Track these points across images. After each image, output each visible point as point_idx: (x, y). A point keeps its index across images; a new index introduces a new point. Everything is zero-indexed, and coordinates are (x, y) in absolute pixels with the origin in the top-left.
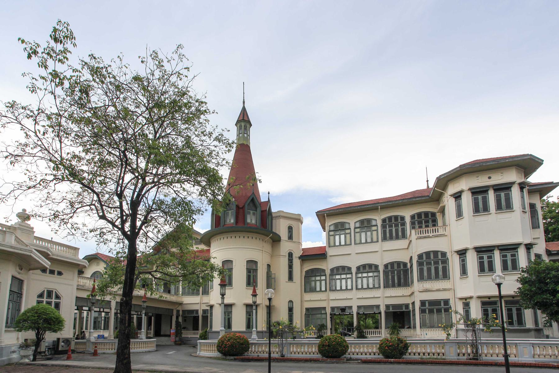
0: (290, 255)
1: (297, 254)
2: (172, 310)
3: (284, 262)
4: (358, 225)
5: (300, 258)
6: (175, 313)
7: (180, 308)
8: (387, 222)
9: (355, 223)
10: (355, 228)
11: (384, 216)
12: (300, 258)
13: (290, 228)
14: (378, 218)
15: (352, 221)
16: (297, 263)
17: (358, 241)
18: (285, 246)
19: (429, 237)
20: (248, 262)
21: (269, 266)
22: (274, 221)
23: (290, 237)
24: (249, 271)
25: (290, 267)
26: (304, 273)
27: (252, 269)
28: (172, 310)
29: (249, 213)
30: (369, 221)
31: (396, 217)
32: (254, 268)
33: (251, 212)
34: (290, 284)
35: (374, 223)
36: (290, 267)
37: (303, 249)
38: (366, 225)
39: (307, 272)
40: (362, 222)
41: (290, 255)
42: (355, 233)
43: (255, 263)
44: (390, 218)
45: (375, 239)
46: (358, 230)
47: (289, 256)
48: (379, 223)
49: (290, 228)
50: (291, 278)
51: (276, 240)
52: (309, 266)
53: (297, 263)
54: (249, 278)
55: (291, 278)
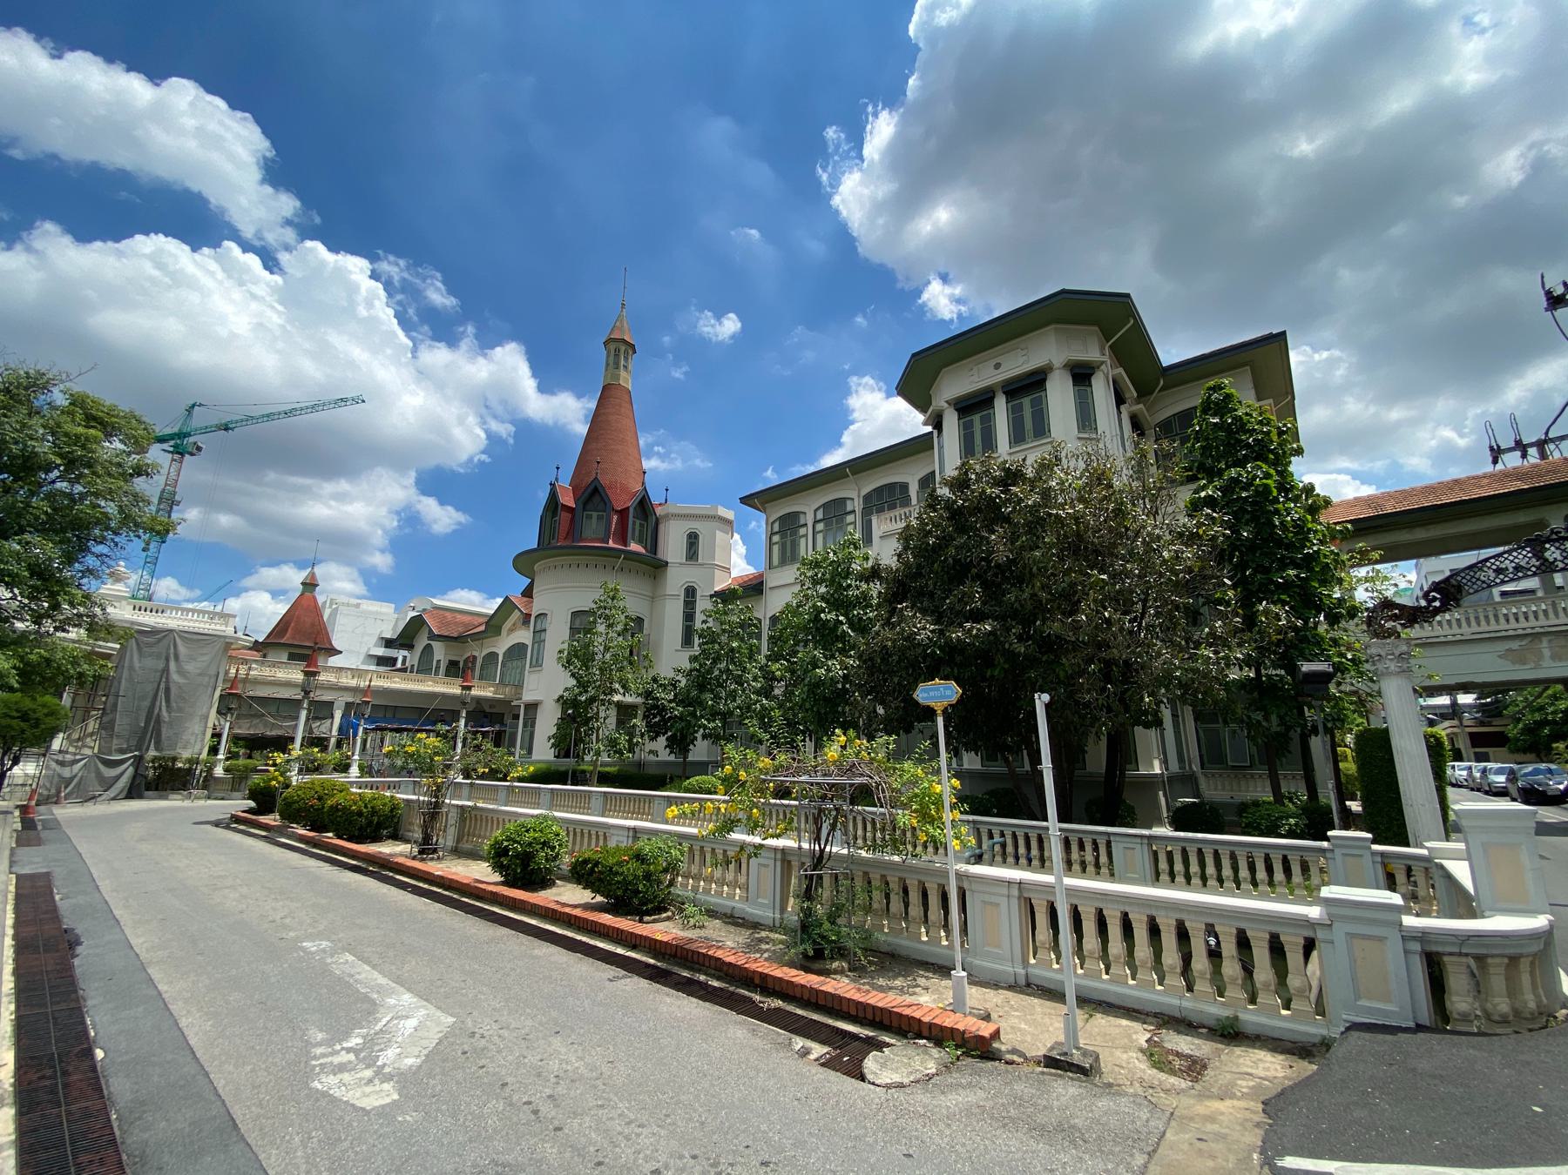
0: (690, 593)
4: (820, 515)
10: (816, 522)
11: (865, 491)
13: (693, 539)
14: (854, 493)
15: (809, 507)
18: (677, 578)
22: (662, 527)
29: (590, 517)
30: (843, 501)
33: (595, 514)
35: (849, 508)
41: (690, 593)
46: (820, 526)
48: (857, 505)
49: (693, 539)
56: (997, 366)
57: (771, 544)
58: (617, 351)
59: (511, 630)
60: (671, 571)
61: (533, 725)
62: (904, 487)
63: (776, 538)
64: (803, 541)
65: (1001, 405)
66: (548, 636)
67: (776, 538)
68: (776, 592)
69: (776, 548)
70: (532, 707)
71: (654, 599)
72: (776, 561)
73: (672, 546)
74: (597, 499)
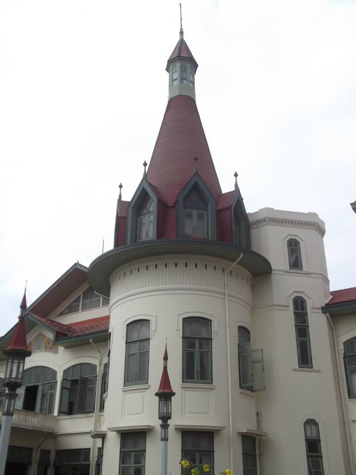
0: (299, 304)
1: (315, 302)
2: (31, 450)
3: (286, 321)
6: (36, 457)
7: (49, 445)
13: (293, 246)
16: (318, 323)
18: (285, 285)
20: (188, 321)
21: (244, 332)
22: (254, 232)
23: (296, 264)
24: (189, 342)
25: (302, 331)
27: (196, 336)
28: (31, 450)
29: (189, 216)
32: (204, 335)
33: (195, 213)
36: (302, 331)
37: (333, 293)
41: (299, 304)
43: (205, 322)
47: (296, 306)
49: (293, 246)
50: (305, 359)
51: (259, 272)
55: (305, 359)
60: (276, 278)
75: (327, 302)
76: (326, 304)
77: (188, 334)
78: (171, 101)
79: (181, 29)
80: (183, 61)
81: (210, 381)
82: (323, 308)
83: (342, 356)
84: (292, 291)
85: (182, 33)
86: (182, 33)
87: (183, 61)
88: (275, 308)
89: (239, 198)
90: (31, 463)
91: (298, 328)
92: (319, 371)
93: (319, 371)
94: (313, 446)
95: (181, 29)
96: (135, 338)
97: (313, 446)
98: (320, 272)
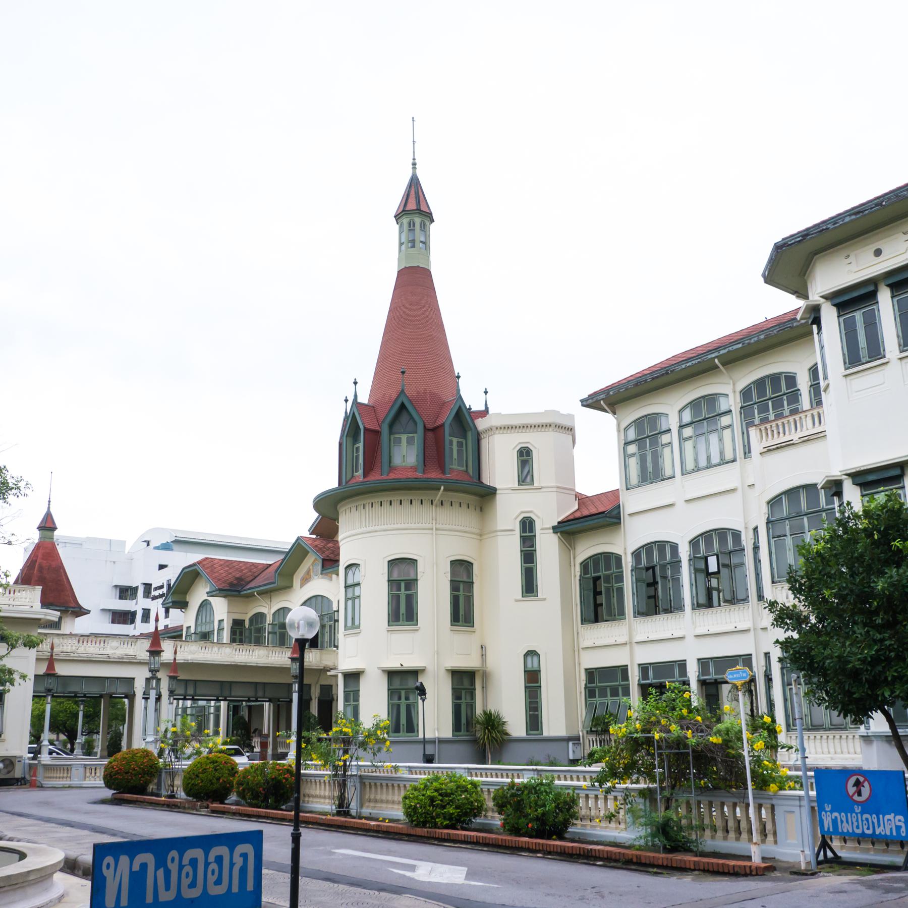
0: (527, 525)
3: (508, 550)
4: (687, 417)
5: (555, 529)
8: (755, 398)
9: (680, 411)
10: (682, 427)
12: (555, 529)
13: (525, 456)
15: (671, 408)
16: (548, 546)
17: (690, 465)
18: (510, 506)
19: (789, 444)
22: (484, 443)
24: (393, 583)
25: (528, 557)
26: (578, 568)
29: (399, 441)
30: (711, 400)
31: (775, 379)
32: (412, 577)
33: (404, 437)
34: (530, 604)
35: (723, 405)
36: (528, 557)
38: (705, 413)
39: (585, 566)
40: (695, 405)
41: (527, 525)
42: (682, 440)
44: (760, 384)
45: (729, 456)
46: (688, 432)
49: (525, 456)
50: (529, 587)
52: (588, 548)
53: (548, 546)
54: (394, 601)
55: (529, 587)
56: (878, 253)
57: (626, 456)
58: (411, 225)
59: (306, 580)
60: (501, 499)
61: (357, 699)
62: (791, 380)
63: (632, 449)
64: (667, 451)
65: (885, 297)
66: (363, 591)
67: (632, 449)
68: (635, 518)
69: (633, 463)
70: (353, 677)
71: (482, 535)
72: (634, 480)
73: (499, 467)
74: (404, 418)
75: (560, 519)
76: (559, 523)
77: (395, 576)
78: (400, 273)
79: (414, 159)
80: (415, 211)
81: (414, 622)
82: (554, 528)
83: (578, 578)
84: (519, 511)
85: (414, 164)
86: (414, 164)
87: (415, 211)
88: (499, 533)
89: (460, 407)
90: (311, 699)
91: (525, 555)
92: (544, 600)
93: (544, 600)
94: (532, 678)
95: (414, 159)
96: (350, 582)
97: (532, 678)
98: (554, 485)
